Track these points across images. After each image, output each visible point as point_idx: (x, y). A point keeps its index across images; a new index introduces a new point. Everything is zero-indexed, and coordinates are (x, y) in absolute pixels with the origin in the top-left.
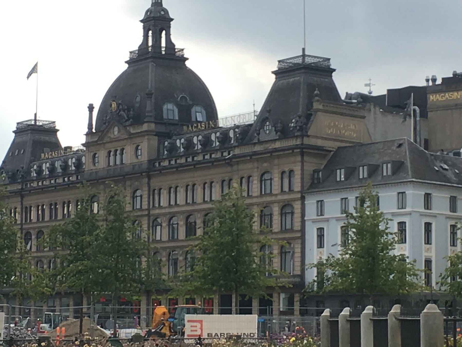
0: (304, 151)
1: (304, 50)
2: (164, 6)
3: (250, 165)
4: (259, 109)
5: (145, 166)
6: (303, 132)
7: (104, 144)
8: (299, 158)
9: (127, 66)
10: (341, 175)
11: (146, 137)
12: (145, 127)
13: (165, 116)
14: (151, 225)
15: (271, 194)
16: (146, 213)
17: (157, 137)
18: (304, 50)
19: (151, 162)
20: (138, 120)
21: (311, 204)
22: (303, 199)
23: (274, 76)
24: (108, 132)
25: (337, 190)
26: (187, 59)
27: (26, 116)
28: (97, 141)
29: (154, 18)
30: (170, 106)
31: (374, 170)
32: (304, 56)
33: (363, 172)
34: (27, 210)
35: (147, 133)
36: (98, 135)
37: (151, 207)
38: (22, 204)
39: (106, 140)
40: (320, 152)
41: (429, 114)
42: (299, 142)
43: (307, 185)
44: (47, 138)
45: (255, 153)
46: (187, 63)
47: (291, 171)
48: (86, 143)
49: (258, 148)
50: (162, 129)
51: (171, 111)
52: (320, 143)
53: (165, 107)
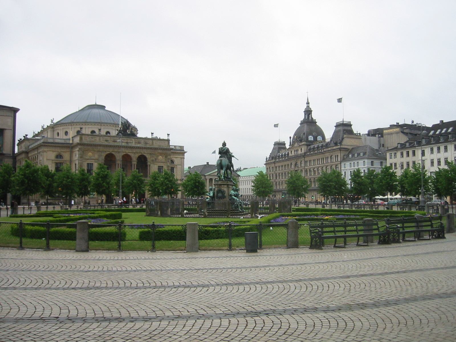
0: (340, 149)
1: (343, 119)
2: (310, 107)
3: (328, 154)
4: (331, 137)
6: (341, 143)
8: (339, 151)
9: (300, 125)
10: (350, 156)
12: (303, 143)
13: (309, 139)
15: (333, 162)
16: (304, 168)
17: (306, 146)
18: (343, 119)
19: (305, 153)
20: (301, 141)
21: (343, 164)
22: (341, 163)
23: (335, 127)
25: (349, 161)
26: (316, 122)
27: (277, 140)
29: (307, 111)
30: (311, 136)
31: (359, 154)
32: (343, 121)
33: (356, 155)
35: (303, 145)
36: (292, 145)
40: (346, 149)
41: (384, 136)
42: (339, 147)
43: (342, 159)
44: (282, 146)
45: (329, 150)
46: (317, 123)
47: (338, 156)
49: (329, 149)
50: (308, 143)
51: (311, 138)
52: (346, 147)
53: (309, 137)
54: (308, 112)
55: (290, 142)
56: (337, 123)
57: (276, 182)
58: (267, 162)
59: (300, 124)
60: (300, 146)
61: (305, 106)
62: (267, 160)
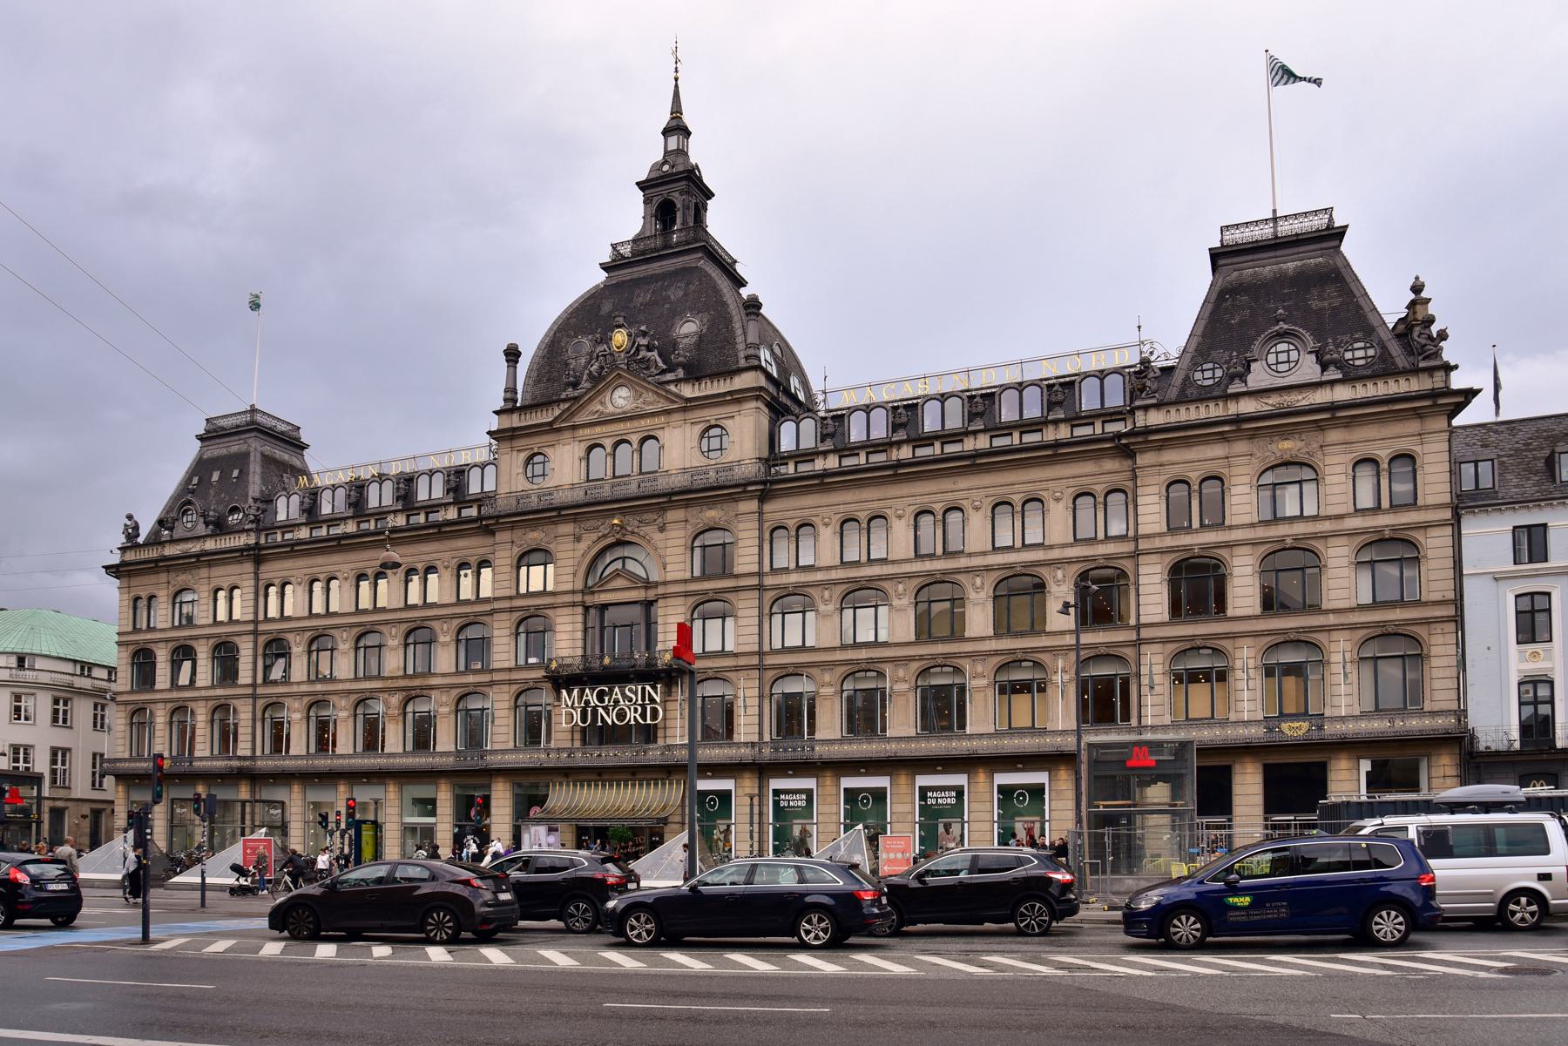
1: (1274, 211)
7: (574, 428)
11: (753, 404)
14: (767, 611)
18: (1274, 211)
24: (591, 400)
28: (550, 424)
34: (261, 592)
37: (767, 568)
38: (257, 579)
39: (581, 419)
45: (1239, 420)
55: (511, 390)
58: (131, 556)
59: (605, 267)
60: (689, 405)
61: (649, 153)
62: (140, 540)
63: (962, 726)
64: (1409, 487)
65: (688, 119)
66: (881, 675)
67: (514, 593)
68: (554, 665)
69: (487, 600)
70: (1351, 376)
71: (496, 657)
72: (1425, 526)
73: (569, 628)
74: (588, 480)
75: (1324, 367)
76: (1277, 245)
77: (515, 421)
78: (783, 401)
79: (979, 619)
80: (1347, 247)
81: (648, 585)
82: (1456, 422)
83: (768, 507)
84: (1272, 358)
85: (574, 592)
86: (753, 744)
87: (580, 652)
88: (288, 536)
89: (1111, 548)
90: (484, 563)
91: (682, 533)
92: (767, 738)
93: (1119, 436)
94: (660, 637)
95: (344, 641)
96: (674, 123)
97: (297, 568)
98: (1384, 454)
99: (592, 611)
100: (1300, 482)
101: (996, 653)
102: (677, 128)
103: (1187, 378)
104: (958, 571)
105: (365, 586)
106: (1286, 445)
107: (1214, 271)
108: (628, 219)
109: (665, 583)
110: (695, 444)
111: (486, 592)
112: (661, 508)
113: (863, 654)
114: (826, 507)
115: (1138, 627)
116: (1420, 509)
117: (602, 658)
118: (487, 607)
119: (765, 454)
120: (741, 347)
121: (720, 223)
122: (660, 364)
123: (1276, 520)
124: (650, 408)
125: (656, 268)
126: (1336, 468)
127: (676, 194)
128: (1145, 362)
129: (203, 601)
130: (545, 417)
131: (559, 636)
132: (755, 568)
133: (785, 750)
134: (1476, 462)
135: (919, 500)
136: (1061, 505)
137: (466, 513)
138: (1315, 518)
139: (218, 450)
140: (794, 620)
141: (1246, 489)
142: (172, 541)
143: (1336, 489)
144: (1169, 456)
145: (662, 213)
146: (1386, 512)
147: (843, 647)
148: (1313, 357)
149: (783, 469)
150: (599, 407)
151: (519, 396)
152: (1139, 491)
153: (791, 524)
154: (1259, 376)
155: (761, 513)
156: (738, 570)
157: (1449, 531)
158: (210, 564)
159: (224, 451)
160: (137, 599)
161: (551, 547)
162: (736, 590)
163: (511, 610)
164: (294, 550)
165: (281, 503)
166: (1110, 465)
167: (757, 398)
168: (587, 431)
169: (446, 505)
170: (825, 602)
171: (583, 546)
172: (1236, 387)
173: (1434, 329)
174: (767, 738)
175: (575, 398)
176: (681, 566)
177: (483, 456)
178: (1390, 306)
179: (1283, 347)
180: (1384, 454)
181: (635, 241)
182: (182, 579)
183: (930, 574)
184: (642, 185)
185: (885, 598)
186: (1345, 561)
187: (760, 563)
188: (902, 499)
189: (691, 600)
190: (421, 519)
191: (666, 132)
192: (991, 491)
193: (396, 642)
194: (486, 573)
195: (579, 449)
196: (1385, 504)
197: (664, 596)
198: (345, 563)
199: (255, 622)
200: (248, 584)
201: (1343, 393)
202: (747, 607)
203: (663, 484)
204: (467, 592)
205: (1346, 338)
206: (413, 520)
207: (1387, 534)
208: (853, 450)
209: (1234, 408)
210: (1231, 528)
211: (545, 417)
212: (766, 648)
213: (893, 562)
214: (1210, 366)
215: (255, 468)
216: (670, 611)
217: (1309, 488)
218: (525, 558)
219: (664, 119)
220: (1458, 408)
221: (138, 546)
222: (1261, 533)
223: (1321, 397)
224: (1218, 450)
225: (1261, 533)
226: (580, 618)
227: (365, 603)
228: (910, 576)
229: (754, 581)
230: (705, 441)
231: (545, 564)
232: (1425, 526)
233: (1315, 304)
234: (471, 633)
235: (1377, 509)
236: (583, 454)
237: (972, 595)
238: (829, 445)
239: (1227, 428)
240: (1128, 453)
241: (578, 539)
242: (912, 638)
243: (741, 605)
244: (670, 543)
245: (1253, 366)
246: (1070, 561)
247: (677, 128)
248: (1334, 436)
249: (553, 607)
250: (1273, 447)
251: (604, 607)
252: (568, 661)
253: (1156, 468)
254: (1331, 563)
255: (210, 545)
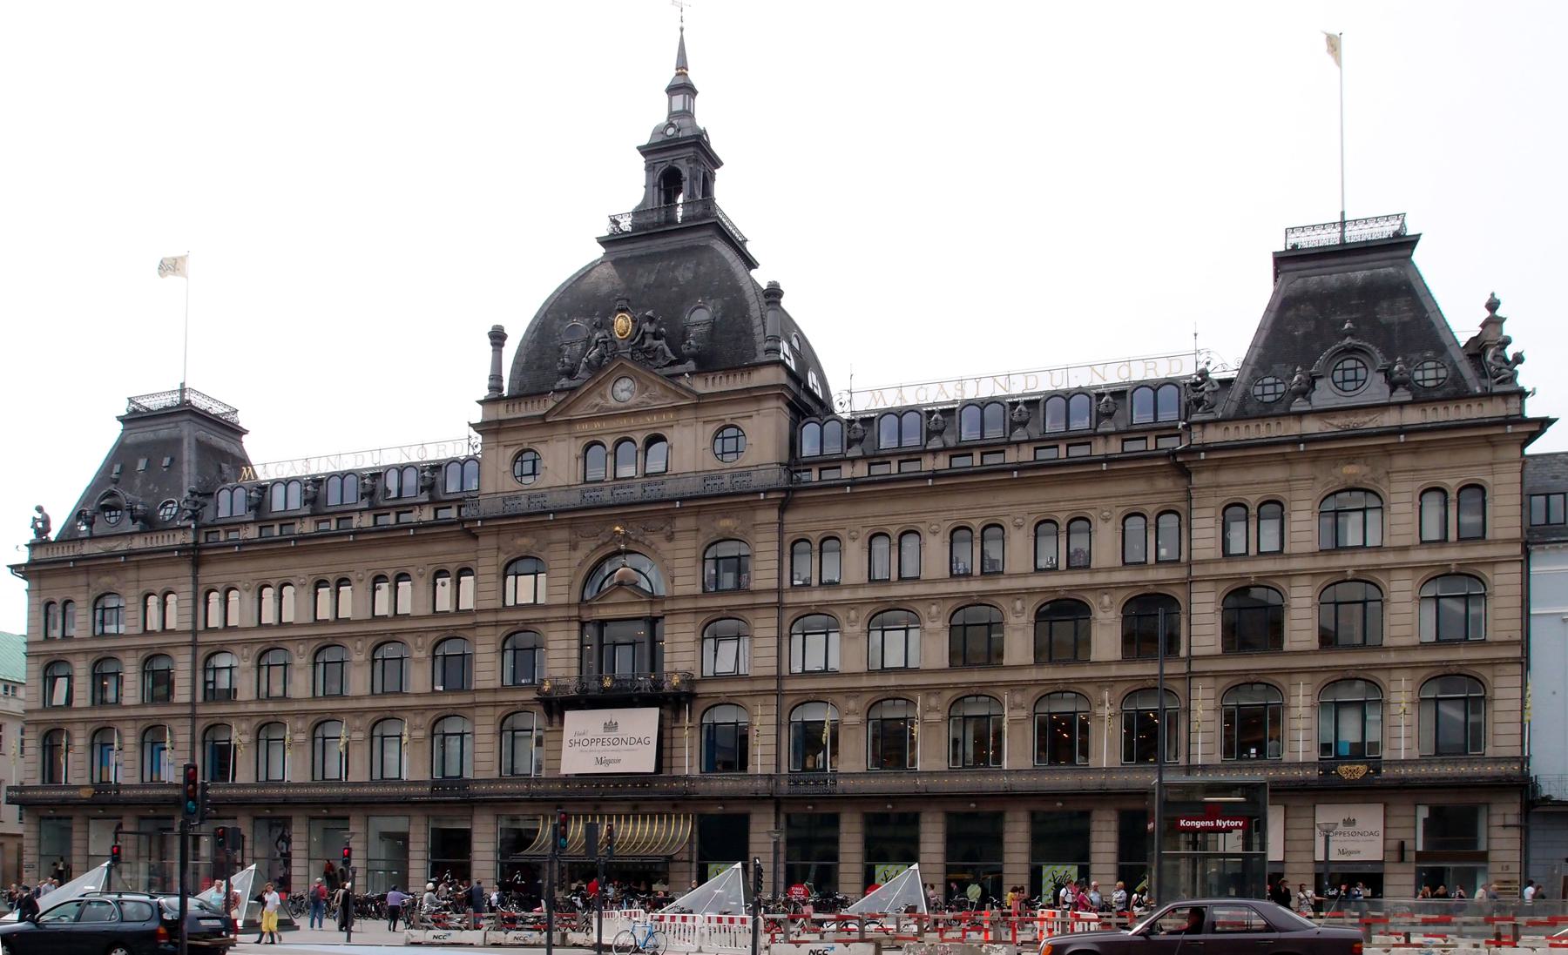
1: (1343, 214)
5: (775, 477)
7: (570, 422)
11: (773, 404)
14: (786, 631)
18: (1343, 214)
28: (543, 417)
34: (200, 598)
38: (196, 583)
39: (577, 413)
48: (483, 423)
54: (680, 161)
55: (496, 377)
56: (1290, 231)
57: (1080, 695)
58: (41, 554)
59: (604, 242)
61: (652, 114)
62: (53, 536)
63: (998, 759)
64: (1478, 519)
65: (694, 77)
66: (911, 703)
67: (500, 604)
68: (547, 687)
69: (468, 612)
70: (1422, 398)
71: (479, 676)
72: (1493, 562)
73: (563, 645)
74: (585, 482)
75: (1394, 386)
76: (1345, 252)
77: (502, 412)
78: (805, 403)
79: (1018, 645)
80: (1419, 257)
81: (653, 599)
82: (1529, 450)
83: (790, 517)
84: (1338, 376)
85: (568, 605)
86: (770, 777)
87: (575, 672)
88: (232, 535)
89: (1162, 574)
90: (465, 571)
91: (692, 543)
92: (784, 770)
93: (1173, 454)
94: (667, 657)
95: (301, 655)
96: (681, 81)
97: (245, 572)
98: (1452, 483)
99: (589, 628)
100: (1364, 510)
101: (1037, 683)
102: (682, 88)
103: (1246, 393)
104: (997, 594)
105: (324, 593)
106: (1349, 470)
107: (1276, 276)
108: (626, 189)
109: (673, 598)
110: (708, 444)
111: (467, 602)
112: (670, 516)
113: (892, 681)
114: (852, 521)
115: (1190, 658)
116: (1489, 543)
117: (600, 680)
118: (468, 621)
119: (786, 459)
120: (759, 338)
121: (732, 196)
122: (669, 354)
123: (1338, 548)
124: (656, 404)
125: (659, 245)
126: (1401, 496)
127: (683, 162)
128: (1204, 374)
129: (130, 608)
130: (536, 409)
131: (551, 654)
132: (774, 584)
133: (806, 783)
134: (1547, 495)
135: (956, 515)
136: (1110, 525)
137: (442, 514)
138: (1379, 549)
139: (145, 434)
140: (816, 642)
141: (1306, 515)
142: (92, 538)
143: (1403, 519)
144: (1226, 476)
145: (666, 182)
146: (1453, 544)
147: (870, 672)
148: (1381, 377)
149: (805, 476)
150: (599, 400)
151: (506, 384)
152: (1194, 514)
153: (815, 537)
154: (1324, 395)
155: (781, 524)
156: (754, 586)
157: (1517, 567)
158: (138, 566)
159: (150, 436)
160: (49, 604)
161: (543, 555)
162: (753, 607)
163: (497, 624)
164: (247, 551)
165: (224, 496)
166: (1163, 484)
167: (779, 396)
168: (585, 427)
169: (420, 505)
170: (851, 623)
171: (579, 555)
172: (1299, 405)
173: (1510, 352)
174: (784, 770)
175: (573, 390)
176: (690, 580)
177: (462, 452)
178: (1463, 324)
179: (1350, 364)
180: (1452, 483)
181: (636, 213)
182: (106, 581)
183: (966, 595)
184: (645, 151)
185: (917, 621)
186: (1408, 596)
187: (780, 578)
188: (937, 517)
189: (702, 618)
190: (391, 519)
191: (672, 90)
192: (1035, 508)
193: (362, 657)
194: (467, 582)
195: (576, 447)
196: (1452, 535)
197: (673, 613)
198: (303, 569)
199: (194, 632)
200: (186, 588)
201: (1412, 417)
202: (765, 628)
203: (670, 488)
204: (444, 603)
205: (1416, 356)
206: (381, 520)
207: (1453, 568)
208: (882, 458)
209: (1292, 428)
210: (1290, 556)
211: (536, 409)
212: (785, 672)
213: (926, 581)
214: (1271, 380)
215: (188, 455)
216: (678, 629)
217: (1373, 516)
218: (509, 568)
219: (668, 75)
220: (1533, 436)
221: (48, 542)
222: (1322, 563)
223: (1390, 419)
224: (1278, 473)
225: (1322, 563)
226: (575, 635)
227: (325, 612)
228: (945, 598)
229: (774, 599)
230: (719, 441)
231: (536, 574)
232: (1493, 562)
233: (1384, 318)
234: (449, 649)
235: (1443, 541)
236: (580, 452)
237: (1011, 620)
238: (855, 451)
239: (1288, 449)
240: (1184, 472)
241: (574, 547)
242: (946, 664)
243: (758, 624)
244: (679, 554)
245: (1318, 383)
246: (1118, 587)
247: (682, 88)
248: (1401, 462)
249: (545, 622)
250: (1336, 471)
251: (602, 624)
252: (563, 682)
253: (1214, 490)
254: (1394, 597)
255: (138, 543)
